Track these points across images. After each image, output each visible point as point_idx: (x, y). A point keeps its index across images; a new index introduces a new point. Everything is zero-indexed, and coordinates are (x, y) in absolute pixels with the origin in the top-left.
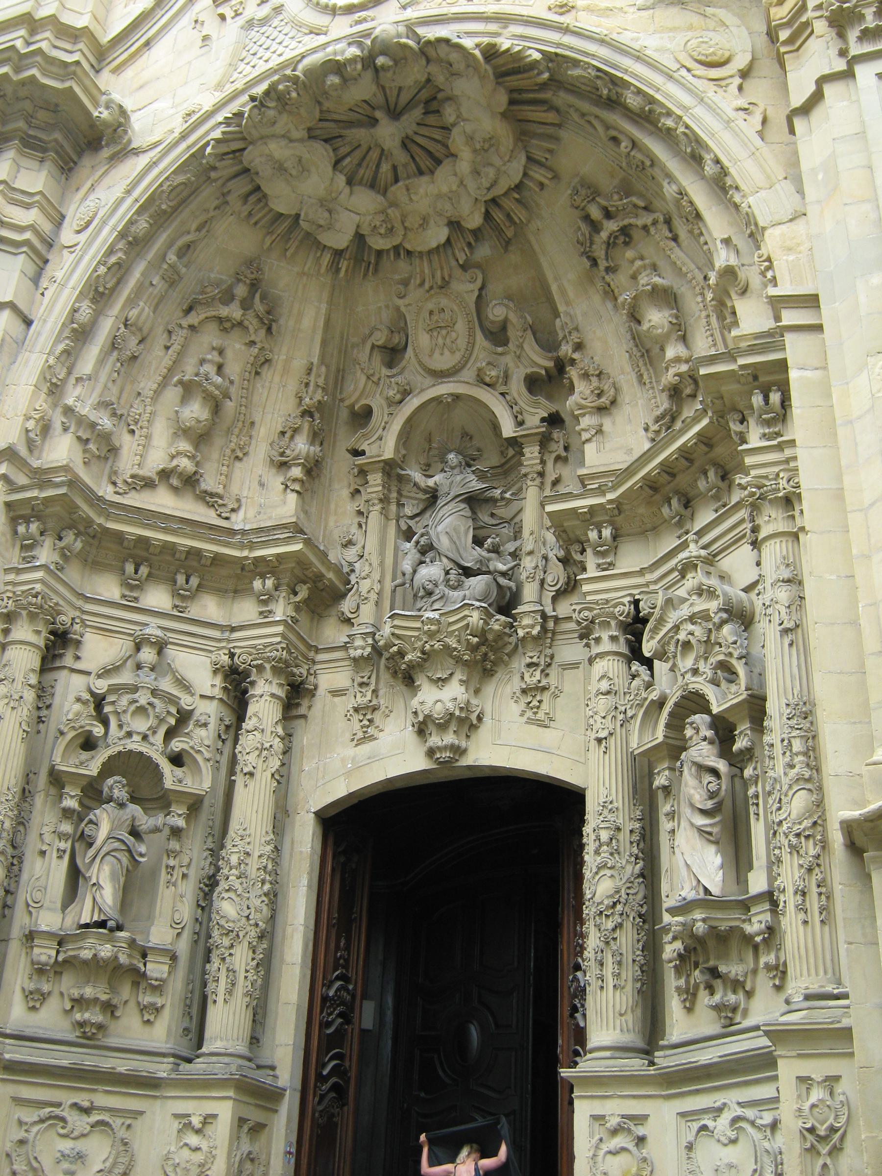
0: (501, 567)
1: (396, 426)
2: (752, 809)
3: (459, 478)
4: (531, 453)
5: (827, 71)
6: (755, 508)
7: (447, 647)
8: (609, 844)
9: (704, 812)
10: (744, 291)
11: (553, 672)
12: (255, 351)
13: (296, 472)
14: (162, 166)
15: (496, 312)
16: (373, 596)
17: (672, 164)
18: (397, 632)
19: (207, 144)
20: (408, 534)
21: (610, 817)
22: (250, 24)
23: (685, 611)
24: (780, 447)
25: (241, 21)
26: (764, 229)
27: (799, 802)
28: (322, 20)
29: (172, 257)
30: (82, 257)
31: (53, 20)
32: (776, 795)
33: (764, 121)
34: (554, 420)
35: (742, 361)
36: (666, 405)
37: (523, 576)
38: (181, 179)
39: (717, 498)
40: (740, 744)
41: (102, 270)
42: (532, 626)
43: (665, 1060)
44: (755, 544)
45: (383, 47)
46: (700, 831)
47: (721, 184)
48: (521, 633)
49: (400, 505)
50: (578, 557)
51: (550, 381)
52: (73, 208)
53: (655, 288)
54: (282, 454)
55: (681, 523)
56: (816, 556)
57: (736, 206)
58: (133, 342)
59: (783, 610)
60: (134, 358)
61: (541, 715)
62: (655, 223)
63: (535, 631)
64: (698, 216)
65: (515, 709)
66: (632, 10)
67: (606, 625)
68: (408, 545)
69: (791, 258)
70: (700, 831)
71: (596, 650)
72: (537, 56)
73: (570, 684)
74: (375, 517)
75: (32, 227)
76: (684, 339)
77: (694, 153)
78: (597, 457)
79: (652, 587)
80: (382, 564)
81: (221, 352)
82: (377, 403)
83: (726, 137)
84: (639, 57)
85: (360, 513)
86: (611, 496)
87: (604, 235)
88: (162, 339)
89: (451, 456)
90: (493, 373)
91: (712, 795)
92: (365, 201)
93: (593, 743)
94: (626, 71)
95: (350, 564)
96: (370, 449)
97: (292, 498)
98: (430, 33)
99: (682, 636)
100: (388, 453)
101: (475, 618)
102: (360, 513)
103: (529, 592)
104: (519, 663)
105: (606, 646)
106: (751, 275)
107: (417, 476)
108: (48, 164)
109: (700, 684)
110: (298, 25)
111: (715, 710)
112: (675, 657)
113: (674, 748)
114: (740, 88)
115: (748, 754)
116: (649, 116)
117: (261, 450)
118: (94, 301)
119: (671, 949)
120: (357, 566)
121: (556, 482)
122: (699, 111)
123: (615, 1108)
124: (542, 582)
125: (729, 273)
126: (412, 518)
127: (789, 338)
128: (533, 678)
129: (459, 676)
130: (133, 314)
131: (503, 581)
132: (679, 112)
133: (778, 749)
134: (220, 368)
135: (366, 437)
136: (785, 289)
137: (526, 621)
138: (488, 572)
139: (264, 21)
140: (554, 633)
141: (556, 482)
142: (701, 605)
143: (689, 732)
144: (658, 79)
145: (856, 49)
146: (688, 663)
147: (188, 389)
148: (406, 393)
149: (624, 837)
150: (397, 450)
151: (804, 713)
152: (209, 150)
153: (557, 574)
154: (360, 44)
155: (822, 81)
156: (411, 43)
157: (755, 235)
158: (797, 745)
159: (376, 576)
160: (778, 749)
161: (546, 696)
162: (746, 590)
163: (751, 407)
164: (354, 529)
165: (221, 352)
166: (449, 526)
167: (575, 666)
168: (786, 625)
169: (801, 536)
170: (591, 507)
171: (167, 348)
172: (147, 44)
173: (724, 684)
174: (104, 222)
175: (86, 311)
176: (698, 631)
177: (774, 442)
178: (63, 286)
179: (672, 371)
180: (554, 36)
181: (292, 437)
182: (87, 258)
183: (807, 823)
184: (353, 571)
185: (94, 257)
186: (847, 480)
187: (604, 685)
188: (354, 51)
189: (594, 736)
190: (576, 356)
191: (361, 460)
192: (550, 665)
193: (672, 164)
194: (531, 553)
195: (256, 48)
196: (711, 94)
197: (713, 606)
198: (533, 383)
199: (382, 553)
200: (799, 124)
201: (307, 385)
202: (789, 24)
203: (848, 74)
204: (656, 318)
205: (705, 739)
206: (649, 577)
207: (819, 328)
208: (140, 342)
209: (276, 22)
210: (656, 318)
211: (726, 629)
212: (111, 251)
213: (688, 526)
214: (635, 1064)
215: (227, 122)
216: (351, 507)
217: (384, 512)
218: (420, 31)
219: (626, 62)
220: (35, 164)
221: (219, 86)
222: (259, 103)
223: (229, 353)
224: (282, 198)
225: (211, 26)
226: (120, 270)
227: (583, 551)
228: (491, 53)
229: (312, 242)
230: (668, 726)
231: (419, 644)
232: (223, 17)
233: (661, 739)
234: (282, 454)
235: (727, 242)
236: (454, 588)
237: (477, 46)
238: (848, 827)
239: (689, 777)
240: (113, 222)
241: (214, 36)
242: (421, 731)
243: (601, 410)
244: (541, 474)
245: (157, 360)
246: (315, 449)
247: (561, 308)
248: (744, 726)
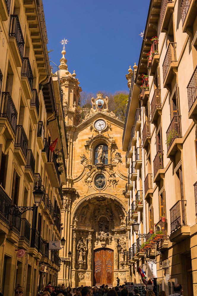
1: (99, 218)
15: (108, 210)
43: (120, 270)
77: (124, 209)
92: (98, 202)
116: (122, 205)
119: (120, 264)
123: (116, 273)
180: (115, 198)
198: (110, 216)
214: (117, 270)
224: (92, 202)
228: (110, 198)
229: (93, 204)
242: (102, 245)
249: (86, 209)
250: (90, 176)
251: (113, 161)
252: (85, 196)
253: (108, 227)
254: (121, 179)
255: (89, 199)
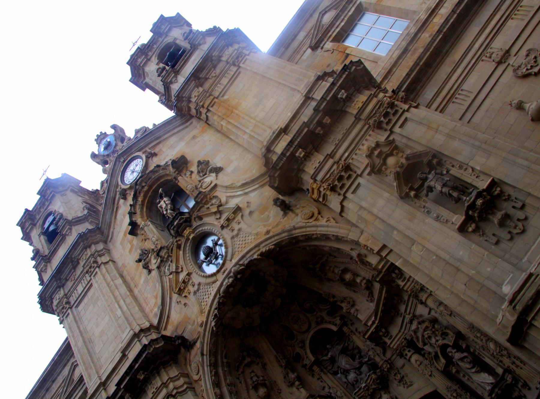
0: (366, 359)
1: (308, 351)
2: (481, 357)
3: (335, 350)
4: (345, 329)
5: (340, 201)
6: (416, 297)
7: (374, 389)
8: (457, 395)
9: (472, 368)
10: (366, 256)
11: (401, 371)
12: (260, 364)
13: (297, 383)
14: (206, 342)
16: (343, 394)
17: (323, 243)
18: (360, 396)
19: (213, 328)
20: (335, 373)
21: (452, 389)
22: (195, 293)
23: (421, 330)
24: (408, 280)
25: (192, 294)
26: (358, 241)
27: (492, 345)
28: (214, 279)
29: (225, 360)
30: (205, 380)
31: (142, 330)
32: (486, 349)
33: (334, 219)
34: (342, 317)
35: (384, 271)
36: (367, 292)
37: (372, 357)
38: (213, 340)
39: (401, 301)
40: (464, 346)
41: (213, 378)
42: (387, 366)
44: (422, 303)
45: (237, 273)
46: (476, 372)
47: (338, 239)
48: (386, 370)
49: (326, 368)
50: (382, 341)
51: (334, 309)
52: (189, 369)
53: (342, 271)
54: (290, 382)
55: (398, 313)
56: (442, 295)
57: (347, 241)
58: (233, 388)
59: (446, 311)
60: (236, 392)
61: (409, 383)
62: (328, 257)
63: (388, 366)
64: (339, 249)
65: (401, 388)
66: (282, 220)
67: (404, 350)
68: (339, 375)
69: (370, 241)
70: (476, 372)
71: (408, 357)
72: (273, 247)
73: (407, 370)
74: (324, 376)
75: (185, 383)
76: (358, 276)
78: (362, 317)
79: (405, 332)
80: (337, 385)
81: (253, 372)
82: (298, 350)
83: (330, 229)
84: (295, 228)
85: (318, 379)
86: (377, 322)
87: (318, 269)
88: (238, 381)
89: (328, 346)
90: (319, 320)
91: (470, 363)
93: (429, 378)
94: (295, 234)
95: (329, 392)
96: (307, 362)
97: (302, 390)
98: (245, 261)
99: (426, 336)
100: (313, 359)
101: (374, 376)
102: (318, 379)
103: (377, 359)
104: (392, 377)
105: (409, 354)
106: (363, 251)
107: (325, 358)
108: (173, 365)
109: (440, 342)
110: (208, 284)
111: (451, 344)
112: (429, 342)
113: (450, 361)
114: (322, 217)
115: (468, 347)
116: (309, 238)
117: (283, 386)
118: (217, 387)
120: (331, 391)
121: (356, 330)
122: (319, 229)
124: (378, 354)
125: (359, 255)
126: (332, 368)
127: (388, 258)
128: (398, 377)
129: (382, 393)
130: (228, 381)
131: (369, 363)
132: (315, 233)
133: (476, 339)
134: (256, 375)
135: (303, 360)
136: (376, 249)
137: (384, 366)
138: (364, 364)
139: (198, 290)
140: (392, 363)
141: (356, 330)
142: (424, 326)
143: (450, 354)
144: (304, 230)
145: (342, 192)
146: (433, 340)
147: (256, 388)
148: (303, 342)
149: (459, 391)
150: (314, 357)
151: (472, 327)
152: (214, 329)
153: (379, 350)
154: (231, 277)
155: (341, 203)
156: (243, 267)
157: (357, 243)
158: (479, 335)
159: (338, 389)
160: (476, 339)
161: (405, 378)
162: (429, 313)
163: (393, 277)
164: (321, 384)
165: (253, 372)
166: (343, 362)
167: (404, 365)
168: (449, 313)
169: (432, 293)
170: (375, 328)
171: (241, 382)
172: (168, 317)
173: (446, 337)
174: (203, 367)
175: (218, 391)
176: (429, 332)
177: (406, 280)
178: (207, 390)
179: (363, 284)
180: (273, 239)
181: (288, 376)
182: (207, 378)
183: (498, 348)
184: (331, 393)
185: (208, 376)
186: (432, 275)
187: (418, 363)
188: (231, 280)
189: (428, 376)
190: (335, 299)
191: (308, 367)
192: (398, 371)
193: (323, 243)
194: (369, 350)
195: (202, 297)
196: (318, 223)
197: (427, 324)
199: (334, 383)
200: (343, 214)
201: (279, 361)
202: (320, 196)
203: (345, 198)
204: (348, 277)
205: (455, 352)
206: (402, 331)
207: (391, 251)
208: (235, 386)
209: (201, 287)
210: (348, 277)
211: (436, 326)
212: (211, 372)
213: (400, 313)
215: (214, 319)
216: (315, 380)
217: (325, 373)
218: (241, 263)
219: (294, 232)
220: (170, 368)
221: (202, 312)
222: (219, 308)
223: (255, 370)
225: (183, 301)
226: (217, 374)
227: (382, 339)
228: (262, 254)
230: (443, 358)
231: (367, 394)
232: (186, 296)
233: (445, 362)
234: (290, 382)
235: (352, 249)
236: (360, 375)
237: (258, 255)
238: (509, 340)
239: (460, 363)
240: (205, 364)
241: (187, 302)
243: (353, 306)
244: (352, 331)
245: (242, 387)
246: (296, 374)
247: (321, 292)
248: (460, 342)
249: (248, 360)
250: (177, 268)
251: (201, 186)
252: (201, 325)
253: (358, 348)
254: (252, 195)
255: (219, 318)
